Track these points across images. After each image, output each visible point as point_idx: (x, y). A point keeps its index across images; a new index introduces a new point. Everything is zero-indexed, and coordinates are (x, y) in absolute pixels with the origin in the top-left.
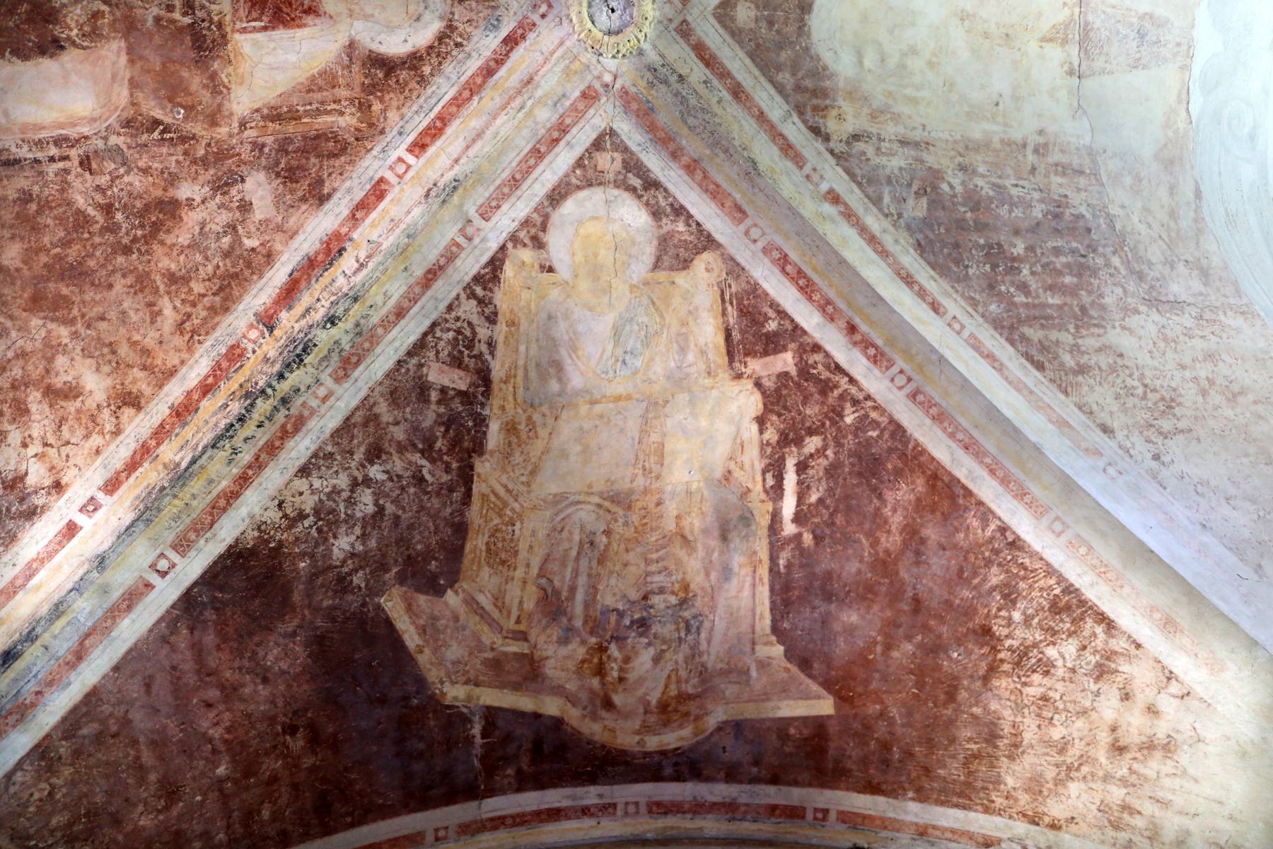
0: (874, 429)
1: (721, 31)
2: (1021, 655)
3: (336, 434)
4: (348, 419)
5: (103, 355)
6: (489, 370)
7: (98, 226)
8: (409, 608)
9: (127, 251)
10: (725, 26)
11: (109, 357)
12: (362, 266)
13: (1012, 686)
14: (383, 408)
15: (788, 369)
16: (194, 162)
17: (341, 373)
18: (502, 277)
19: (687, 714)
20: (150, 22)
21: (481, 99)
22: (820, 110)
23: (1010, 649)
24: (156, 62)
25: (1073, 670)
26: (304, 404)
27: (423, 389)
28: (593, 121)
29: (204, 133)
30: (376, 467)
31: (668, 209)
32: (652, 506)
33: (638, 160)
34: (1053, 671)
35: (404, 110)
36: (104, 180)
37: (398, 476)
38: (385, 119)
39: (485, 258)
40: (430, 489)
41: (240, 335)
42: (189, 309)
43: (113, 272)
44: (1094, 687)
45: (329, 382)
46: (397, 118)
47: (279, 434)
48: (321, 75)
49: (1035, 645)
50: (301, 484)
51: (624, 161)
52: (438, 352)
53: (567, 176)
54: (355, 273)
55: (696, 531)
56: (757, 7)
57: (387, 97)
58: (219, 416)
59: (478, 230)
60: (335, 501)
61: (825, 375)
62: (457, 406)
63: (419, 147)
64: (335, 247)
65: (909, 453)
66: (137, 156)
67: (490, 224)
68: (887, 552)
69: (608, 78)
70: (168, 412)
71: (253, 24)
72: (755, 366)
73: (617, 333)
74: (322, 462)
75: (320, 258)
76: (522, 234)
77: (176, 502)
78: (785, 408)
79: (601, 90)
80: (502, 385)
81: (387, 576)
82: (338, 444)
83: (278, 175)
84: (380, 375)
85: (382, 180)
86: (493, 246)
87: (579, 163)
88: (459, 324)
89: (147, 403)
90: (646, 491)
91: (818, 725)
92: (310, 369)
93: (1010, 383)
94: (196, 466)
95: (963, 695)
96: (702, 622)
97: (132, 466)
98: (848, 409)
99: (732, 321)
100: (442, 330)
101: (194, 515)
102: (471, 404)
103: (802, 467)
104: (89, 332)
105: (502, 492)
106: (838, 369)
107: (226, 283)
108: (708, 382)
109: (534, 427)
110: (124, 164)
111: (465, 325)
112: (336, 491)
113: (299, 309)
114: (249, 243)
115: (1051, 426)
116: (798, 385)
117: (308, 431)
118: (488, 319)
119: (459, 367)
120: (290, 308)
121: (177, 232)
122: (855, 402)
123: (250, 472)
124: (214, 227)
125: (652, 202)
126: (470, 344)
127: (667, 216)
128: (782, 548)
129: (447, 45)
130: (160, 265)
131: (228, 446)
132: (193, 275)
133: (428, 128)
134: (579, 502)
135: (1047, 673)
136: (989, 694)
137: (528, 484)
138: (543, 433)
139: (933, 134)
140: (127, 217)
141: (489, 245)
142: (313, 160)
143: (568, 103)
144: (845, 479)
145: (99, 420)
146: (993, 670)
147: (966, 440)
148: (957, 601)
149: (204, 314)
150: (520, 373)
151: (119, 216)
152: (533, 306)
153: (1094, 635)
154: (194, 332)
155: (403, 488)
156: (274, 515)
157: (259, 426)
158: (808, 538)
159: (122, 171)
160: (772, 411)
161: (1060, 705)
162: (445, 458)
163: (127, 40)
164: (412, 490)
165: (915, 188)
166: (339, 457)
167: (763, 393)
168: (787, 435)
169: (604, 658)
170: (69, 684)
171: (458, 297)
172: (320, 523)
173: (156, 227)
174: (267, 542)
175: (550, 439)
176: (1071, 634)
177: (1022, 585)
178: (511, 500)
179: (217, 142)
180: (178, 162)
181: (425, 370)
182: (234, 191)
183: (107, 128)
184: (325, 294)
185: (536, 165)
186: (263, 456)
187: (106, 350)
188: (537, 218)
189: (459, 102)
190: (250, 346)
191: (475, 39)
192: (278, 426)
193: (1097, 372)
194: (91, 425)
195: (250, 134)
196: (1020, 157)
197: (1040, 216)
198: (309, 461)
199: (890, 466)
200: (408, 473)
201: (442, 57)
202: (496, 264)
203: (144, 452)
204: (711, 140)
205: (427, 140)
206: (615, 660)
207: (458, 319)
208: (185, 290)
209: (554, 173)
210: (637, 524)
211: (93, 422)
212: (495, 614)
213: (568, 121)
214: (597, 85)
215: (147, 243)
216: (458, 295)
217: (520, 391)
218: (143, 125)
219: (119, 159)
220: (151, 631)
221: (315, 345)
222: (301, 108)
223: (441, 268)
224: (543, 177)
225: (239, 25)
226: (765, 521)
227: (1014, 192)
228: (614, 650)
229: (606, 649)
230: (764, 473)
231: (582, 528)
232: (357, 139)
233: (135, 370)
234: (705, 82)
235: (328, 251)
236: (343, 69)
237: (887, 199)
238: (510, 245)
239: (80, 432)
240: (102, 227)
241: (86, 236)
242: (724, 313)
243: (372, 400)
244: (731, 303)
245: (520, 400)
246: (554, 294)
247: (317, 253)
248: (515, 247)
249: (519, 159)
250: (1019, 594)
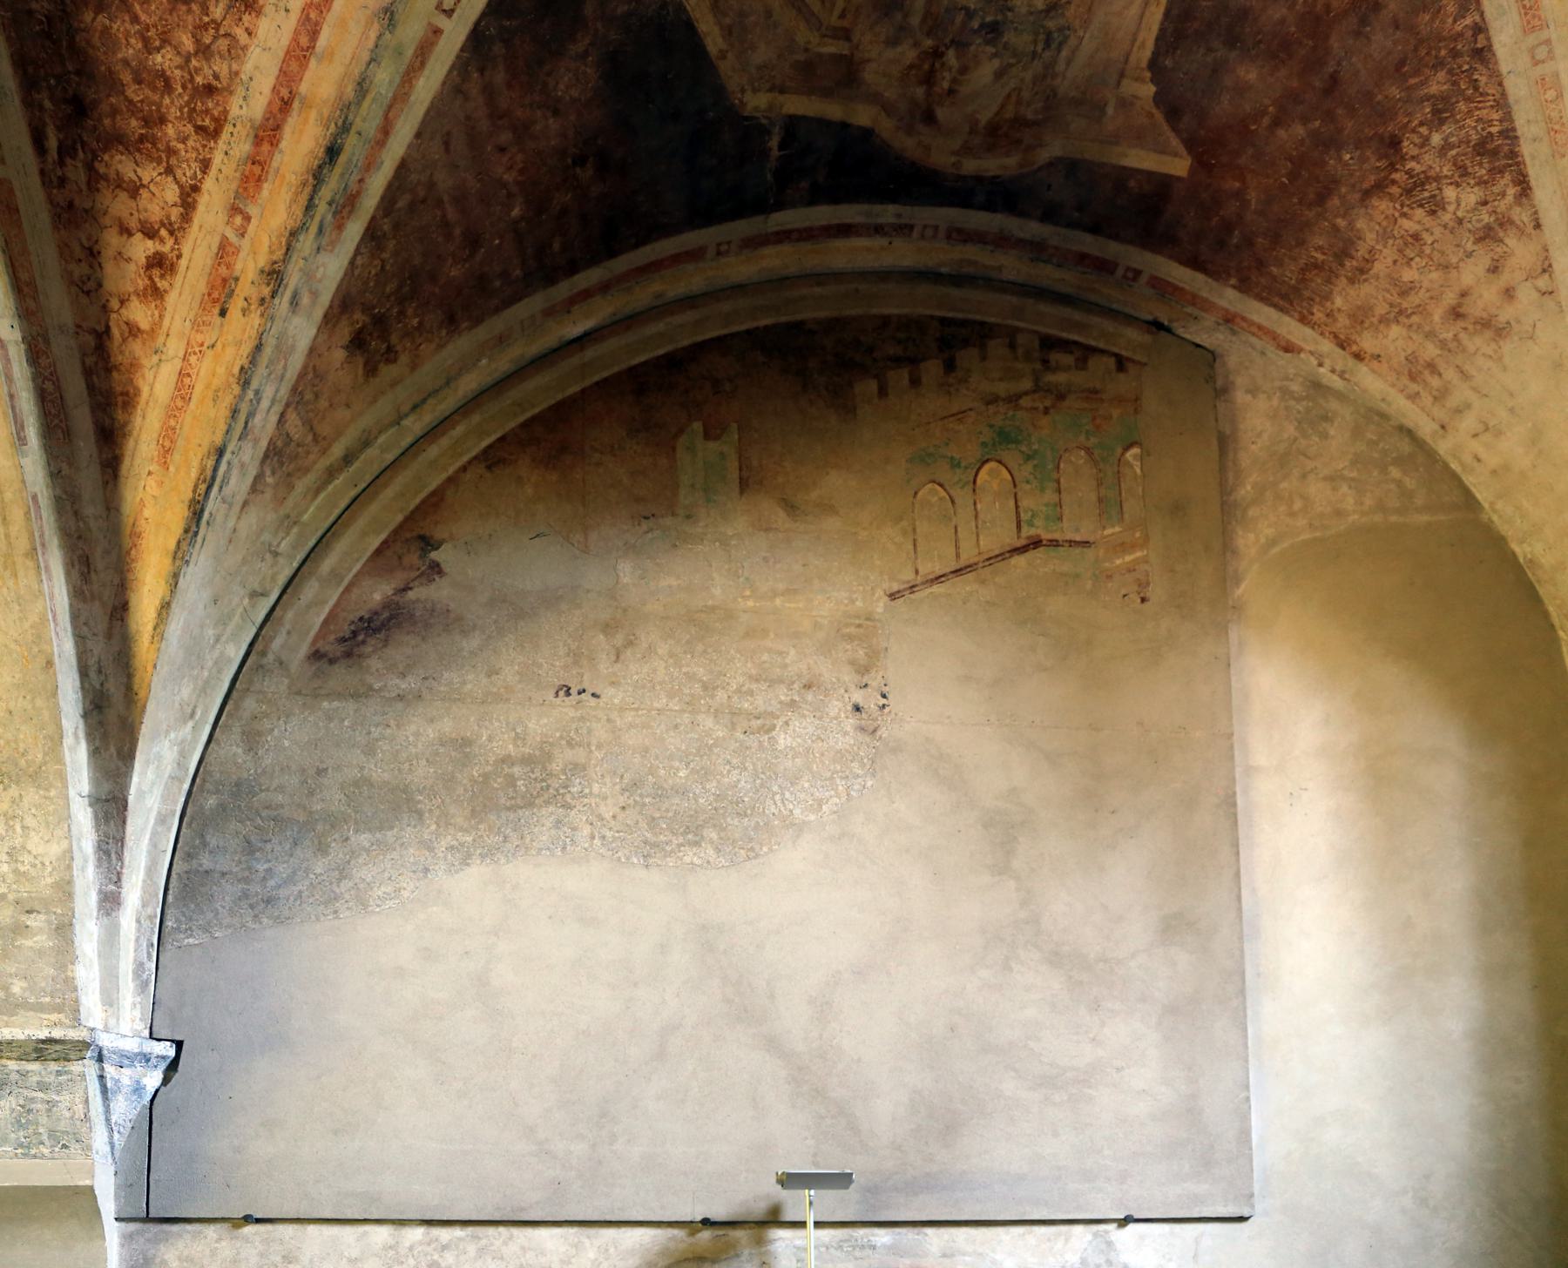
2: (1419, 183)
19: (1019, 142)
23: (1409, 173)
34: (1439, 213)
49: (1437, 179)
96: (1067, 38)
136: (1363, 211)
146: (1380, 187)
148: (1379, 97)
176: (1481, 183)
229: (942, 55)
250: (1453, 116)
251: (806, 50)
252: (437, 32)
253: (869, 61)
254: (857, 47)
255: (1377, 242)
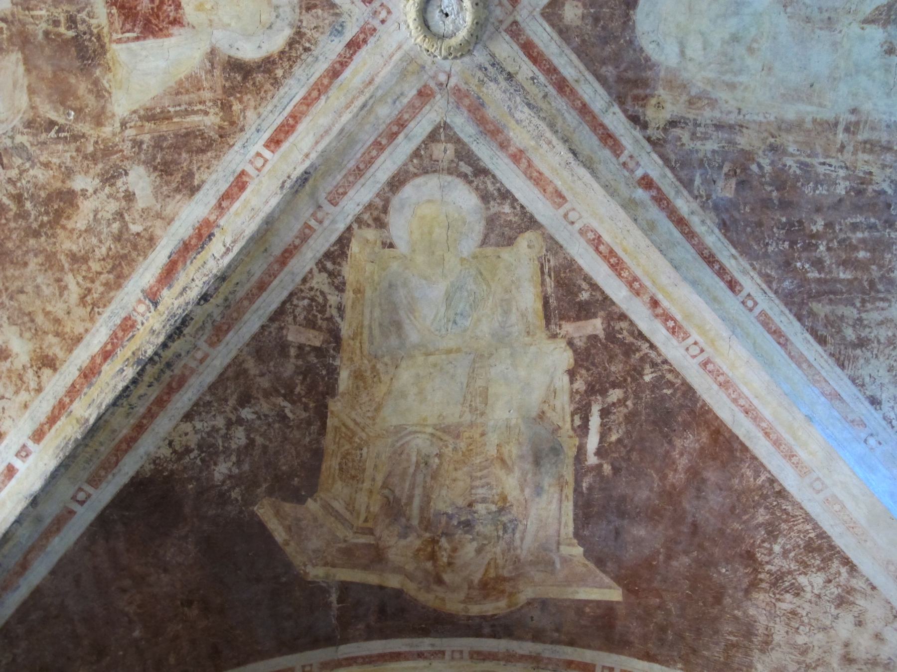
0: (668, 388)
1: (549, 29)
2: (777, 579)
3: (212, 388)
4: (222, 374)
5: (24, 323)
6: (339, 330)
7: (12, 214)
8: (277, 513)
9: (36, 234)
10: (553, 25)
11: (29, 325)
12: (228, 250)
13: (768, 600)
14: (250, 364)
15: (597, 332)
16: (85, 157)
17: (215, 339)
18: (349, 253)
19: (503, 592)
20: (40, 36)
21: (328, 98)
22: (642, 100)
23: (769, 572)
24: (48, 70)
25: (819, 596)
26: (185, 366)
27: (283, 347)
28: (429, 116)
29: (92, 132)
30: (247, 409)
31: (496, 193)
32: (477, 436)
33: (469, 150)
34: (802, 594)
35: (261, 110)
36: (13, 173)
37: (266, 416)
38: (245, 118)
39: (334, 238)
40: (291, 424)
41: (131, 309)
42: (89, 285)
43: (27, 252)
44: (834, 611)
45: (204, 347)
46: (255, 117)
47: (166, 391)
48: (187, 79)
49: (790, 572)
50: (187, 427)
51: (456, 151)
52: (295, 317)
53: (405, 164)
54: (222, 257)
55: (514, 456)
56: (585, 6)
57: (245, 98)
58: (118, 379)
59: (327, 214)
60: (214, 438)
61: (629, 339)
62: (313, 359)
63: (274, 142)
64: (205, 232)
65: (697, 410)
66: (38, 152)
67: (338, 208)
68: (673, 486)
69: (442, 78)
70: (77, 373)
71: (127, 35)
72: (568, 328)
73: (449, 299)
74: (202, 409)
75: (193, 242)
76: (366, 217)
77: (88, 449)
78: (593, 364)
79: (436, 88)
80: (351, 342)
81: (259, 490)
82: (214, 394)
83: (155, 169)
84: (247, 337)
85: (243, 173)
86: (341, 227)
87: (416, 154)
88: (312, 293)
89: (61, 365)
90: (471, 425)
91: (608, 608)
92: (188, 338)
93: (792, 357)
94: (102, 421)
95: (727, 601)
97: (52, 420)
98: (648, 369)
99: (549, 290)
100: (298, 299)
101: (103, 457)
102: (325, 357)
103: (605, 413)
104: (12, 303)
105: (351, 425)
106: (641, 336)
107: (117, 262)
108: (527, 339)
109: (378, 374)
110: (29, 159)
111: (318, 294)
112: (215, 430)
113: (178, 287)
114: (135, 228)
115: (823, 399)
116: (606, 347)
117: (190, 386)
118: (337, 288)
119: (314, 328)
120: (170, 287)
121: (75, 218)
122: (654, 365)
123: (145, 421)
124: (105, 214)
125: (481, 187)
126: (323, 309)
127: (495, 200)
128: (585, 474)
129: (296, 50)
130: (64, 247)
131: (125, 404)
132: (90, 255)
133: (282, 125)
134: (416, 432)
135: (797, 595)
136: (749, 603)
137: (373, 419)
138: (385, 378)
139: (747, 117)
140: (35, 206)
141: (337, 226)
142: (184, 155)
143: (405, 101)
144: (641, 426)
145: (25, 379)
146: (754, 585)
147: (747, 406)
149: (101, 289)
150: (366, 332)
151: (28, 205)
152: (376, 278)
153: (839, 573)
154: (94, 305)
155: (269, 425)
156: (166, 452)
157: (149, 386)
158: (607, 469)
159: (28, 165)
160: (581, 366)
161: (806, 620)
162: (304, 399)
163: (23, 53)
164: (277, 425)
165: (725, 169)
166: (216, 404)
167: (575, 351)
168: (593, 387)
169: (436, 548)
170: (19, 587)
171: (311, 271)
172: (203, 455)
173: (59, 214)
174: (161, 472)
175: (391, 383)
177: (784, 526)
178: (359, 430)
179: (103, 140)
180: (72, 157)
181: (285, 332)
182: (119, 183)
183: (13, 129)
184: (198, 275)
185: (378, 156)
186: (154, 408)
187: (26, 319)
188: (379, 203)
189: (308, 101)
190: (139, 319)
191: (321, 44)
192: (165, 384)
193: (875, 344)
194: (19, 383)
195: (130, 133)
196: (831, 137)
197: (843, 192)
198: (192, 409)
199: (680, 419)
200: (273, 413)
201: (292, 61)
202: (343, 242)
203: (60, 409)
204: (535, 133)
205: (282, 136)
206: (445, 550)
207: (311, 289)
208: (84, 267)
209: (394, 163)
210: (464, 450)
211: (21, 379)
212: (348, 515)
213: (406, 116)
214: (432, 84)
215: (52, 228)
216: (311, 270)
217: (366, 346)
218: (41, 125)
219: (25, 155)
220: (76, 543)
221: (192, 319)
222: (172, 109)
223: (296, 247)
224: (384, 166)
225: (115, 36)
226: (572, 452)
227: (821, 170)
228: (444, 542)
230: (572, 415)
231: (419, 452)
232: (221, 136)
233: (50, 336)
234: (533, 79)
235: (200, 236)
236: (206, 73)
237: (698, 181)
238: (355, 226)
239: (11, 389)
240: (16, 214)
241: (3, 221)
242: (543, 283)
243: (241, 358)
244: (550, 276)
245: (366, 352)
246: (395, 266)
247: (191, 238)
248: (360, 227)
249: (362, 151)
251: (345, 541)
252: (72, 513)
253: (389, 547)
254: (380, 538)
255: (769, 622)
